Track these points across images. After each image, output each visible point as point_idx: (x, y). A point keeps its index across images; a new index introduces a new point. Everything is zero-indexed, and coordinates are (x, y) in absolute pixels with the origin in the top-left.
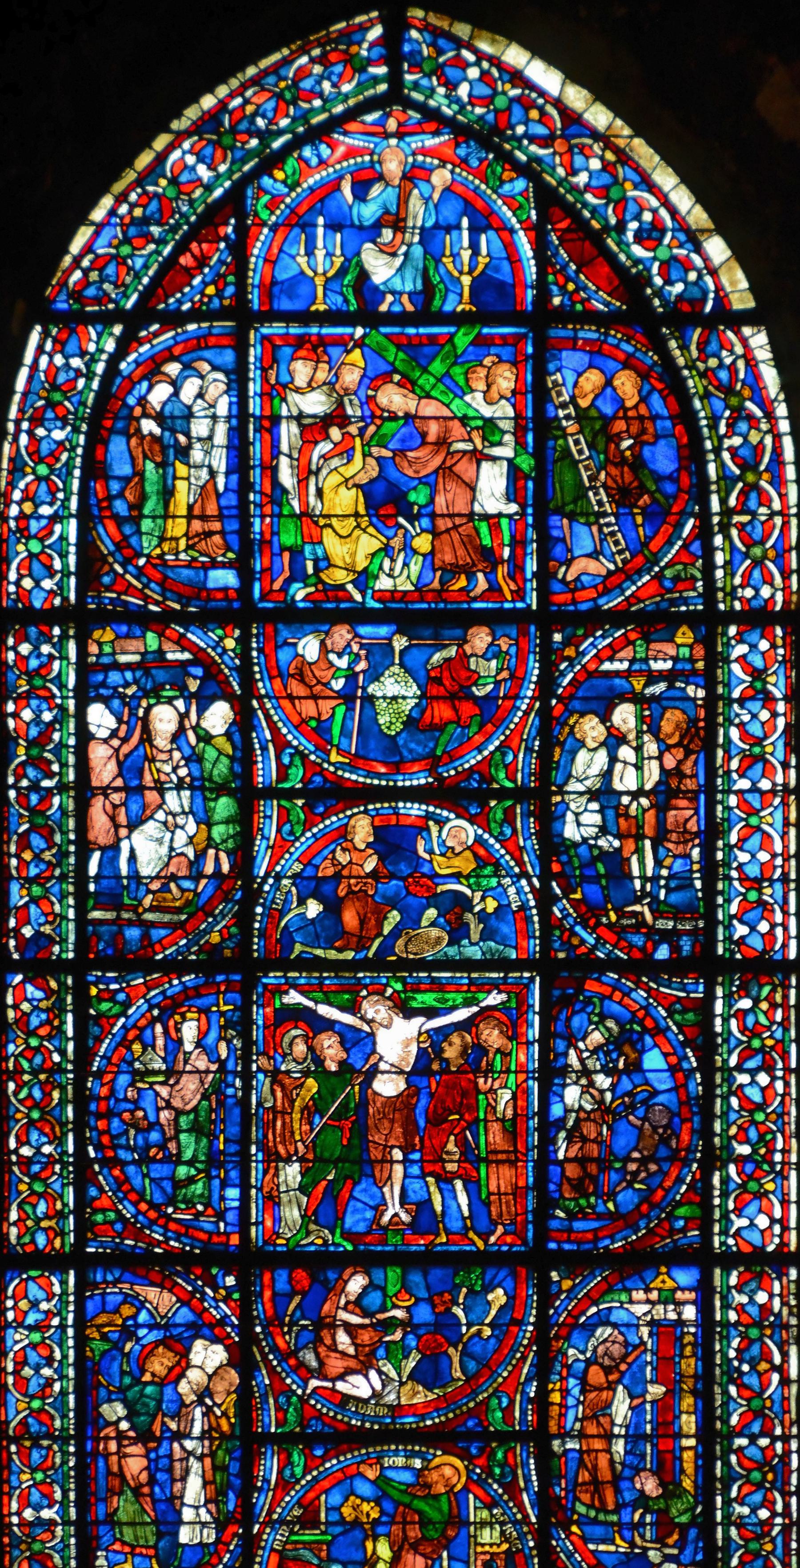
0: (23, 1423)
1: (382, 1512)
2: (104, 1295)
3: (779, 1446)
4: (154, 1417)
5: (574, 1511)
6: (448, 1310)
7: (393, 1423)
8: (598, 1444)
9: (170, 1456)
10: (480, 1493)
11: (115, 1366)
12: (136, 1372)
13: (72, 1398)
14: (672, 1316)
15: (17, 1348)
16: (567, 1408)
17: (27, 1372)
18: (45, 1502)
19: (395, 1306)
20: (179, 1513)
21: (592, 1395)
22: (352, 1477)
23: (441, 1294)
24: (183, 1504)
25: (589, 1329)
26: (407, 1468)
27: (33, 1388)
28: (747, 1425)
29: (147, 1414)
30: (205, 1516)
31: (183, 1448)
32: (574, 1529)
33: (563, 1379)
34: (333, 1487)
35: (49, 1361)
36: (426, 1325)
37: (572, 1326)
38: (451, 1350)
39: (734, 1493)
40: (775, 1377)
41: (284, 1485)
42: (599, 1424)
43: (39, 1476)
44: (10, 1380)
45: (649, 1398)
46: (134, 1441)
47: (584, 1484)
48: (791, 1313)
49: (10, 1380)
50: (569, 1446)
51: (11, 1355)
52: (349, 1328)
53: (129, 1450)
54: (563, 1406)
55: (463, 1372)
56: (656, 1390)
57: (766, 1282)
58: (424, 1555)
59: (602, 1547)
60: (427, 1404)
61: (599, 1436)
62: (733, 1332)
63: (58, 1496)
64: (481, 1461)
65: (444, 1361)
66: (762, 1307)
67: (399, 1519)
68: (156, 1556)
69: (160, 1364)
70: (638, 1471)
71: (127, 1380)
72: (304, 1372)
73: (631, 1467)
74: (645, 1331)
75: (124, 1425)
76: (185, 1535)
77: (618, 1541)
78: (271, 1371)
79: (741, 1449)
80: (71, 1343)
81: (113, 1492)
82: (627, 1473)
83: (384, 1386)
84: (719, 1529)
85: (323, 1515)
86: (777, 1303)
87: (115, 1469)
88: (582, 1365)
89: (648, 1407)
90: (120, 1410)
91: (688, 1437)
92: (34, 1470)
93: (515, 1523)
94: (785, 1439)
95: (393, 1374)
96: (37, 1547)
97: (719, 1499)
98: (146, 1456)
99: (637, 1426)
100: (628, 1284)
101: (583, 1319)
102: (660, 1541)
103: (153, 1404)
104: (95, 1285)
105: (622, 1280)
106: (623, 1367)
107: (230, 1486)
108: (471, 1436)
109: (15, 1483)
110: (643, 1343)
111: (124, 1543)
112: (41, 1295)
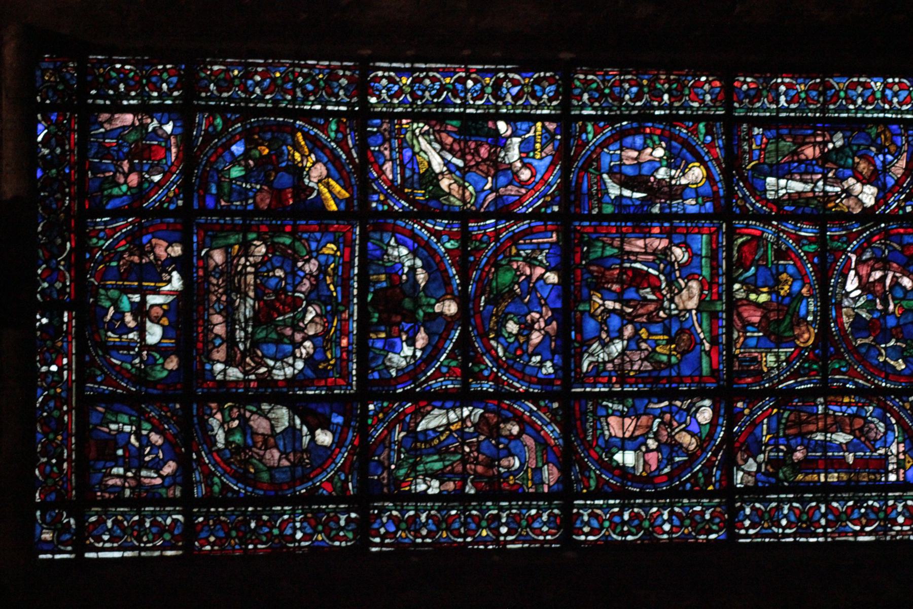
0: (832, 87)
1: (783, 297)
2: (901, 135)
3: (820, 530)
4: (835, 163)
5: (785, 410)
6: (893, 337)
7: (832, 304)
8: (821, 424)
9: (814, 173)
10: (794, 355)
11: (862, 141)
12: (860, 153)
13: (845, 115)
14: (891, 467)
15: (872, 83)
16: (841, 406)
17: (860, 89)
18: (789, 99)
19: (895, 305)
20: (783, 178)
21: (847, 421)
22: (802, 279)
23: (902, 332)
24: (788, 180)
25: (884, 419)
26: (808, 313)
27: (851, 93)
28: (832, 513)
29: (837, 159)
30: (783, 192)
31: (819, 180)
32: (775, 411)
33: (856, 404)
34: (798, 268)
35: (865, 103)
36: (886, 322)
37: (886, 409)
38: (871, 338)
39: (795, 505)
40: (858, 528)
41: (798, 240)
42: (832, 425)
43: (803, 95)
44: (855, 80)
45: (846, 454)
46: (822, 152)
47: (800, 416)
48: (892, 536)
49: (855, 80)
50: (820, 408)
51: (869, 80)
52: (883, 278)
53: (817, 148)
54: (842, 404)
55: (860, 345)
56: (850, 458)
57: (909, 522)
58: (760, 321)
59: (765, 426)
60: (842, 324)
61: (826, 425)
62: (882, 503)
63: (793, 106)
64: (811, 355)
65: (865, 334)
66: (895, 519)
67: (780, 307)
68: (759, 164)
69: (863, 166)
70: (806, 447)
71: (855, 148)
72: (859, 252)
73: (809, 443)
74: (882, 451)
75: (831, 146)
76: (771, 180)
77: (769, 437)
78: (860, 233)
79: (819, 508)
80: (875, 115)
81: (794, 138)
82: (806, 441)
83: (853, 298)
84: (775, 496)
85: (782, 262)
86: (898, 528)
87: (807, 140)
88: (864, 415)
89: (841, 454)
90: (839, 144)
91: (826, 477)
92: (806, 92)
93: (779, 376)
94: (825, 534)
95: (859, 304)
96: (765, 93)
97: (791, 496)
98: (814, 158)
99: (831, 447)
100: (907, 441)
101: (889, 415)
102: (769, 462)
103: (842, 163)
104: (906, 131)
105: (909, 438)
106: (863, 439)
107: (798, 207)
108: (825, 349)
109: (800, 81)
110: (875, 451)
111: (767, 144)
112: (901, 98)
